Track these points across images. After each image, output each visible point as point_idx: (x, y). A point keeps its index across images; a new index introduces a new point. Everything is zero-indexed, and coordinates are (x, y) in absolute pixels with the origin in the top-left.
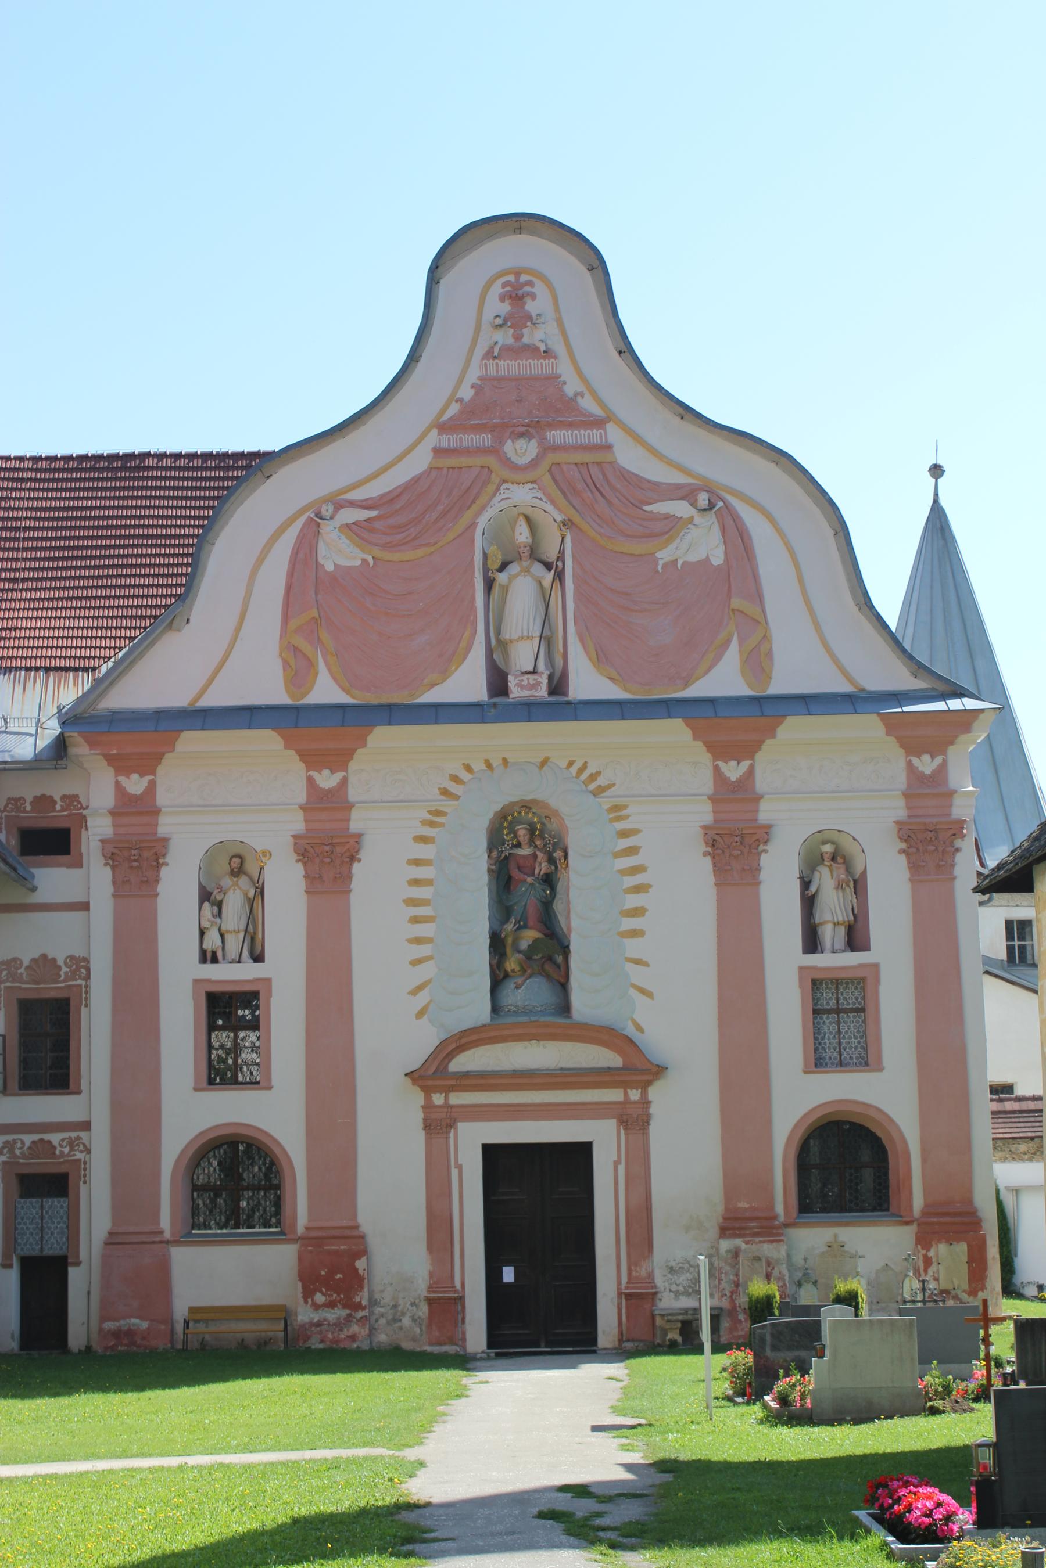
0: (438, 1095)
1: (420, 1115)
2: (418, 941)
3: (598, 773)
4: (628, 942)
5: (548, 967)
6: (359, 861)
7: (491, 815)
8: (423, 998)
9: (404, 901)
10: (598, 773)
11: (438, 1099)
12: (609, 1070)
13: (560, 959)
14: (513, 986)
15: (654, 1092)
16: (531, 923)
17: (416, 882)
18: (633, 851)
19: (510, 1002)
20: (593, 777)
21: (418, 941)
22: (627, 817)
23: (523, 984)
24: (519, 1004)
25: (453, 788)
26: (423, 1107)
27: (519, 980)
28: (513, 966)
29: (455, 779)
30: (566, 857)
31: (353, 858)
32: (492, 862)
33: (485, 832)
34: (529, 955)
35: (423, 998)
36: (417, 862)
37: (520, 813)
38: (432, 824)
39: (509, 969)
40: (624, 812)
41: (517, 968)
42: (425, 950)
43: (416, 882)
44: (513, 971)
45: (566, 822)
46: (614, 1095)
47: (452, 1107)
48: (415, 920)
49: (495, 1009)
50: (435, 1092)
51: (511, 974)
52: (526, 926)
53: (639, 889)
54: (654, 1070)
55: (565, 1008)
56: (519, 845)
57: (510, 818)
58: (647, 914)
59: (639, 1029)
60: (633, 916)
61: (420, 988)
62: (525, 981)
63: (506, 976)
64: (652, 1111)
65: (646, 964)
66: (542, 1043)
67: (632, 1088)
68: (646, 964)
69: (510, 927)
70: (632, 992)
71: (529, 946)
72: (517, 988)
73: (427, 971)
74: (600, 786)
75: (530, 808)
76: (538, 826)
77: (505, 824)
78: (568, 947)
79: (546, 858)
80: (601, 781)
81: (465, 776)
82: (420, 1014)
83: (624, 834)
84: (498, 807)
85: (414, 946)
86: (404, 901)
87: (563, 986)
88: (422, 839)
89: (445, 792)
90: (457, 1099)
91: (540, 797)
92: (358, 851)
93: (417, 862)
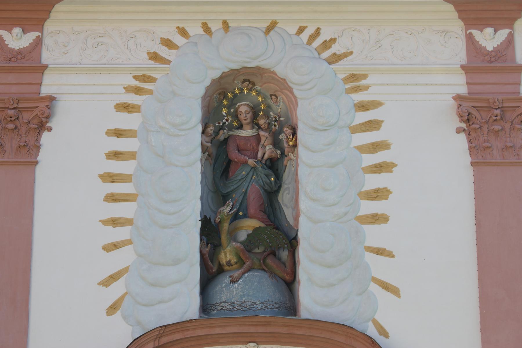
5: (270, 261)
6: (50, 130)
9: (100, 176)
14: (227, 280)
19: (224, 299)
24: (234, 300)
27: (236, 274)
31: (42, 125)
33: (200, 101)
34: (249, 245)
36: (118, 133)
39: (224, 261)
41: (234, 260)
44: (229, 263)
51: (227, 268)
62: (243, 274)
71: (249, 235)
72: (233, 282)
83: (363, 107)
88: (125, 108)
92: (48, 117)
93: (118, 133)
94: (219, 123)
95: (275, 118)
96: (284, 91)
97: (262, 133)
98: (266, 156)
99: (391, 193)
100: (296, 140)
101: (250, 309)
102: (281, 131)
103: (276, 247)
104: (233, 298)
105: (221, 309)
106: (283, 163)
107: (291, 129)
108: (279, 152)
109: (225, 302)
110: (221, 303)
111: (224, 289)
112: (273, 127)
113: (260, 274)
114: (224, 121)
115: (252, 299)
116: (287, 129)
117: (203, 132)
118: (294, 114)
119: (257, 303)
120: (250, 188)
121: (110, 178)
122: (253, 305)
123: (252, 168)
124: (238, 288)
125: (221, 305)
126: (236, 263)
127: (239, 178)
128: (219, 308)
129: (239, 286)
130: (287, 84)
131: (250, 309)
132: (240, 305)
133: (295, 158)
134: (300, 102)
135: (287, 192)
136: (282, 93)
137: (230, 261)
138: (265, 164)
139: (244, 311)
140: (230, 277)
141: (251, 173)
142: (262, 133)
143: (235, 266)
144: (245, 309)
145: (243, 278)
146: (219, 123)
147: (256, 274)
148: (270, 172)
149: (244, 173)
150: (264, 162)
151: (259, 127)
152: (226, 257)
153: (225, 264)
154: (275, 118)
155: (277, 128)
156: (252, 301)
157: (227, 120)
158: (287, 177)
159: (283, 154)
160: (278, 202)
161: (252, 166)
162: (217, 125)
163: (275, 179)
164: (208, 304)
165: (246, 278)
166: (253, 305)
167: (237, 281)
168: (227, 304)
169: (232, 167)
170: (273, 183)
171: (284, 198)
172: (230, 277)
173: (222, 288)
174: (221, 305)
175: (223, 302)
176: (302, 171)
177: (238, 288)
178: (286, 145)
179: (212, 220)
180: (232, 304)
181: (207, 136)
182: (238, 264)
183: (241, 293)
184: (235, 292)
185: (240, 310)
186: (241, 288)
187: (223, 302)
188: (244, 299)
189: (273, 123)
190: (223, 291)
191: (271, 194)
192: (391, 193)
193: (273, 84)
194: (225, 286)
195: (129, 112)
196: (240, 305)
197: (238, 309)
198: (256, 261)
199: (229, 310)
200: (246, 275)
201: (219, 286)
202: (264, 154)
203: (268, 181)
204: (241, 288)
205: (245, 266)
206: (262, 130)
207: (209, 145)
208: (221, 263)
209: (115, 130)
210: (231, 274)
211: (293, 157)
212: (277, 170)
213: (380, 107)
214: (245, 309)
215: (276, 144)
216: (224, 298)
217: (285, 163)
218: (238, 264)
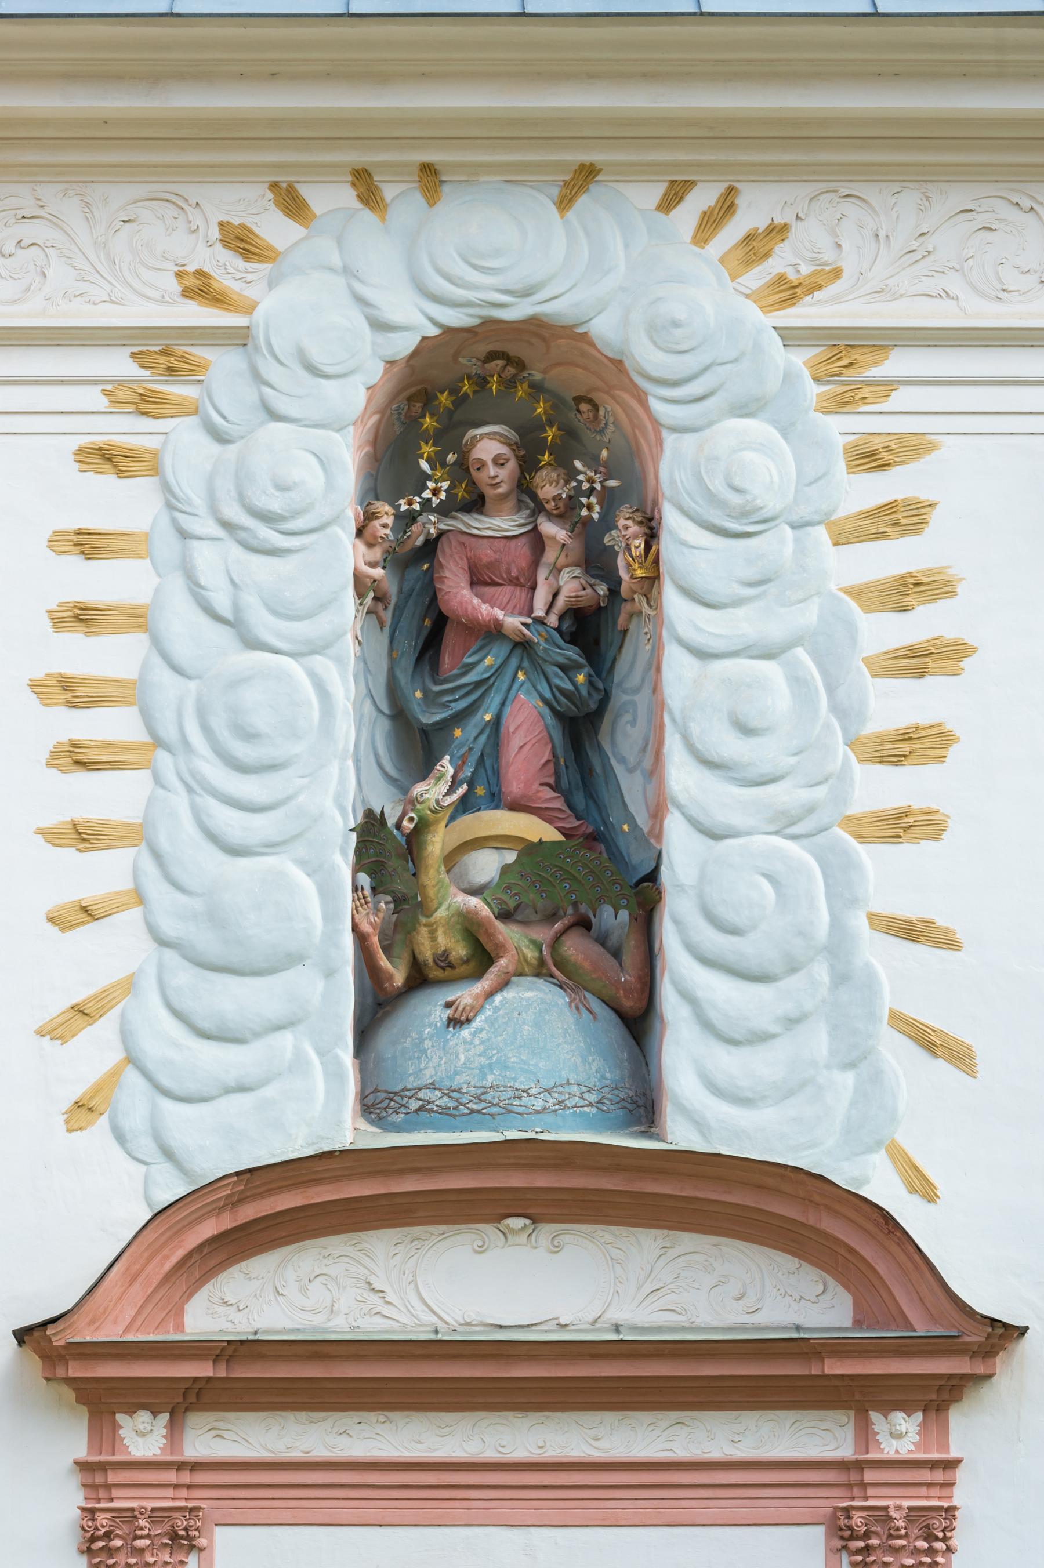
0: (143, 1418)
1: (68, 1500)
2: (83, 836)
3: (778, 231)
4: (873, 860)
7: (375, 372)
8: (94, 1052)
9: (35, 686)
10: (778, 231)
11: (143, 1437)
12: (798, 1347)
13: (615, 919)
14: (440, 1015)
15: (967, 1431)
16: (514, 785)
17: (83, 617)
18: (901, 518)
20: (756, 246)
21: (83, 836)
22: (888, 386)
23: (478, 1009)
24: (459, 1080)
25: (226, 269)
26: (84, 1466)
27: (466, 994)
28: (443, 941)
29: (241, 242)
30: (652, 536)
32: (377, 554)
35: (94, 1052)
36: (88, 544)
37: (482, 382)
38: (146, 404)
39: (426, 953)
40: (874, 373)
41: (460, 950)
42: (105, 872)
43: (83, 617)
44: (444, 960)
45: (655, 405)
46: (817, 1438)
47: (195, 1466)
48: (76, 758)
49: (373, 1105)
50: (131, 1410)
51: (435, 973)
52: (496, 800)
53: (915, 662)
54: (975, 1337)
55: (643, 1106)
56: (477, 504)
57: (444, 398)
58: (953, 752)
59: (923, 1188)
60: (899, 760)
61: (82, 1013)
62: (490, 994)
63: (419, 979)
64: (959, 1497)
65: (948, 942)
66: (547, 1230)
67: (887, 1407)
68: (948, 942)
69: (433, 792)
70: (895, 1052)
71: (505, 870)
72: (456, 1022)
73: (116, 949)
74: (781, 279)
75: (520, 365)
76: (550, 434)
77: (428, 421)
78: (653, 876)
79: (575, 547)
80: (784, 260)
81: (274, 228)
82: (83, 1110)
84: (404, 345)
85: (69, 855)
86: (35, 686)
87: (637, 1022)
89: (200, 288)
90: (212, 1439)
91: (558, 305)
93: (88, 544)
94: (410, 503)
95: (591, 481)
96: (618, 392)
97: (549, 528)
98: (561, 603)
99: (956, 740)
100: (657, 561)
101: (510, 1112)
102: (608, 523)
103: (598, 907)
104: (456, 1073)
105: (420, 1109)
106: (615, 623)
107: (640, 523)
108: (602, 589)
109: (432, 1086)
110: (420, 1089)
111: (428, 1044)
112: (584, 512)
113: (541, 995)
114: (427, 494)
115: (515, 1079)
116: (629, 523)
117: (360, 533)
118: (651, 470)
119: (532, 1092)
120: (507, 710)
121: (68, 691)
122: (520, 1098)
123: (517, 645)
124: (471, 1043)
125: (421, 1095)
126: (467, 962)
127: (472, 677)
128: (414, 1105)
129: (474, 1034)
130: (632, 381)
131: (510, 1112)
132: (479, 1099)
133: (652, 613)
134: (670, 440)
135: (627, 717)
136: (613, 397)
137: (446, 954)
138: (558, 630)
139: (491, 1115)
140: (448, 1005)
141: (514, 662)
142: (549, 528)
143: (461, 970)
144: (495, 1110)
145: (488, 1011)
146: (410, 503)
147: (530, 994)
148: (572, 653)
149: (488, 661)
150: (553, 620)
151: (539, 508)
152: (433, 938)
153: (430, 961)
154: (591, 481)
155: (596, 516)
156: (517, 1085)
157: (435, 492)
158: (629, 667)
159: (614, 592)
160: (600, 749)
161: (518, 639)
162: (404, 508)
163: (591, 683)
164: (376, 1091)
165: (497, 1009)
166: (520, 1098)
167: (468, 1021)
168: (438, 1093)
169: (450, 638)
170: (584, 692)
171: (622, 740)
172: (448, 1005)
173: (421, 1040)
174: (421, 1095)
175: (426, 1087)
176: (678, 671)
177: (471, 1043)
178: (623, 574)
179: (391, 822)
180: (455, 1095)
181: (370, 545)
182: (472, 964)
183: (483, 1060)
184: (462, 1058)
185: (478, 1112)
186: (482, 1042)
187: (426, 1087)
188: (490, 1078)
189: (584, 500)
190: (425, 1051)
191: (579, 730)
192: (956, 740)
193: (585, 369)
194: (431, 1037)
195: (120, 473)
196: (479, 1099)
197: (472, 1111)
198: (531, 954)
199: (444, 1111)
200: (498, 998)
201: (414, 1035)
202: (555, 596)
203: (570, 687)
204: (482, 1042)
205: (494, 970)
206: (550, 516)
207: (378, 572)
208: (420, 957)
209: (79, 533)
210: (450, 999)
211: (646, 609)
212: (597, 642)
213: (928, 458)
214: (495, 1110)
215: (597, 561)
216: (428, 1073)
217: (621, 620)
218: (472, 964)
